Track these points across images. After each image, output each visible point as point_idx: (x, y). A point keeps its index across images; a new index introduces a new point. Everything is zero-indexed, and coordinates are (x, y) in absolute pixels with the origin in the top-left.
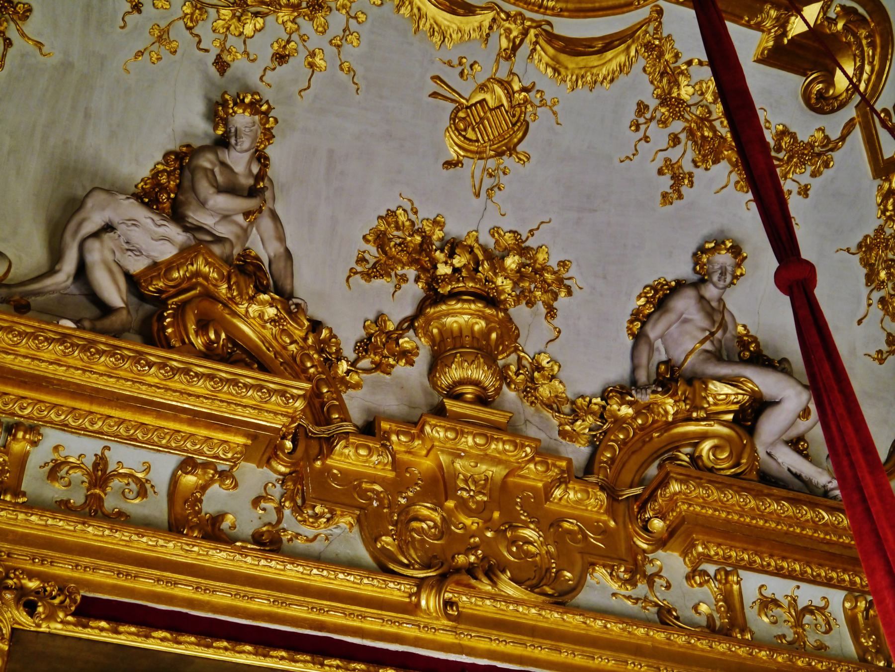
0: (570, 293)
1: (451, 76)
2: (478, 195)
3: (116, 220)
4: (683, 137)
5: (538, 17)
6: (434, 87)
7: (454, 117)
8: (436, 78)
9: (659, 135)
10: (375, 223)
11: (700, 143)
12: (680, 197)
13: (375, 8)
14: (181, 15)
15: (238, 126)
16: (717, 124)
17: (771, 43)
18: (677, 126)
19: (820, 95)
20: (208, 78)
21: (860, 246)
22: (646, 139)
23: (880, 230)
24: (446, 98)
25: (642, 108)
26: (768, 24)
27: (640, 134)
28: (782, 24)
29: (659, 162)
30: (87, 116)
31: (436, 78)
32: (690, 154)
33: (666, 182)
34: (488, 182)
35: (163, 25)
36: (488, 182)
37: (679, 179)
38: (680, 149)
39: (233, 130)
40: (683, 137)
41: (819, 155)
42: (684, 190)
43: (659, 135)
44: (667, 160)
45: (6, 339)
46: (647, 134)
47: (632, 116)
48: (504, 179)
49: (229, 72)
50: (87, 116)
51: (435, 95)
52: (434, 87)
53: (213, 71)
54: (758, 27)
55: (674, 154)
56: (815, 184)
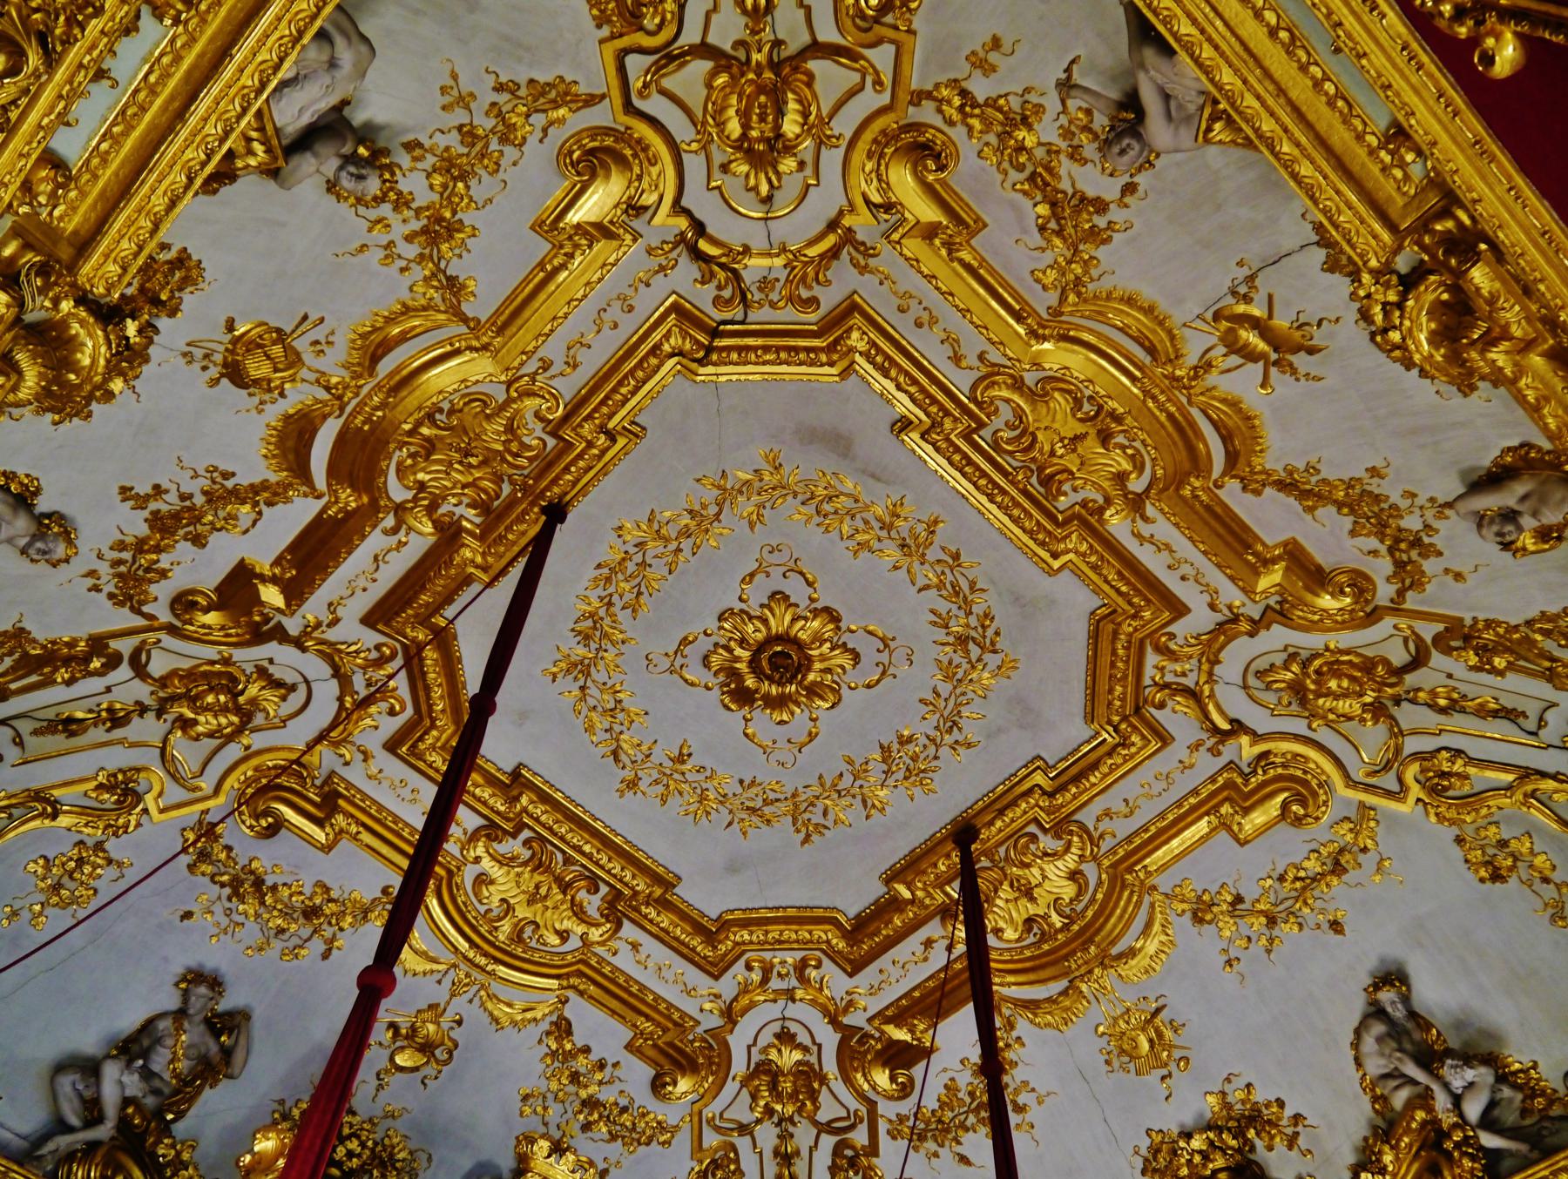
0: (55, 423)
1: (319, 333)
2: (188, 345)
3: (338, 74)
4: (188, 503)
5: (349, 409)
6: (313, 317)
7: (279, 331)
8: (322, 320)
9: (195, 487)
10: (195, 257)
11: (176, 516)
12: (124, 500)
13: (409, 283)
14: (475, 123)
15: (369, 181)
16: (191, 528)
17: (258, 570)
18: (199, 500)
19: (194, 605)
20: (406, 131)
21: (22, 630)
22: (196, 476)
23: (34, 641)
24: (297, 327)
25: (227, 475)
26: (277, 571)
27: (201, 472)
28: (274, 580)
29: (165, 485)
30: (417, 12)
31: (322, 320)
32: (164, 508)
33: (143, 488)
34: (198, 353)
35: (473, 106)
36: (198, 353)
37: (141, 502)
38: (177, 501)
39: (364, 172)
40: (188, 503)
41: (131, 598)
42: (132, 503)
43: (195, 487)
44: (167, 491)
45: (305, 5)
46: (748, 1138)
47: (222, 467)
48: (196, 366)
49: (403, 151)
50: (417, 12)
51: (305, 318)
52: (313, 317)
53: (410, 137)
54: (277, 562)
55: (172, 497)
56: (102, 597)
